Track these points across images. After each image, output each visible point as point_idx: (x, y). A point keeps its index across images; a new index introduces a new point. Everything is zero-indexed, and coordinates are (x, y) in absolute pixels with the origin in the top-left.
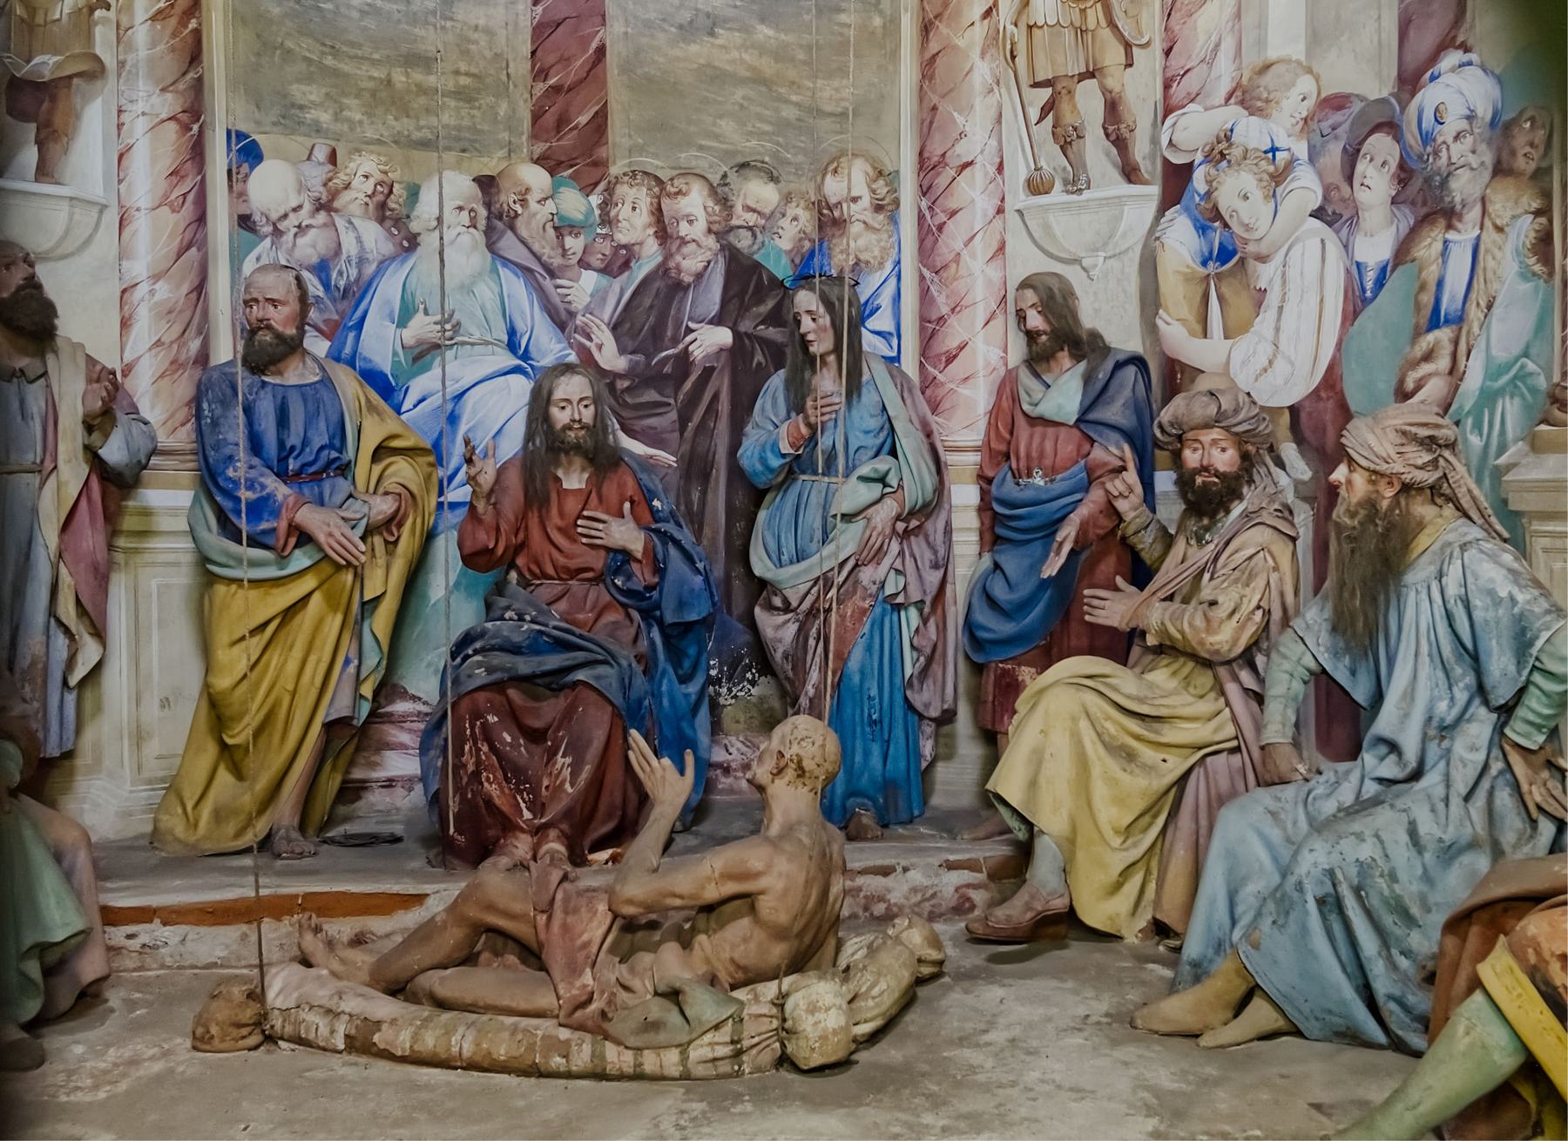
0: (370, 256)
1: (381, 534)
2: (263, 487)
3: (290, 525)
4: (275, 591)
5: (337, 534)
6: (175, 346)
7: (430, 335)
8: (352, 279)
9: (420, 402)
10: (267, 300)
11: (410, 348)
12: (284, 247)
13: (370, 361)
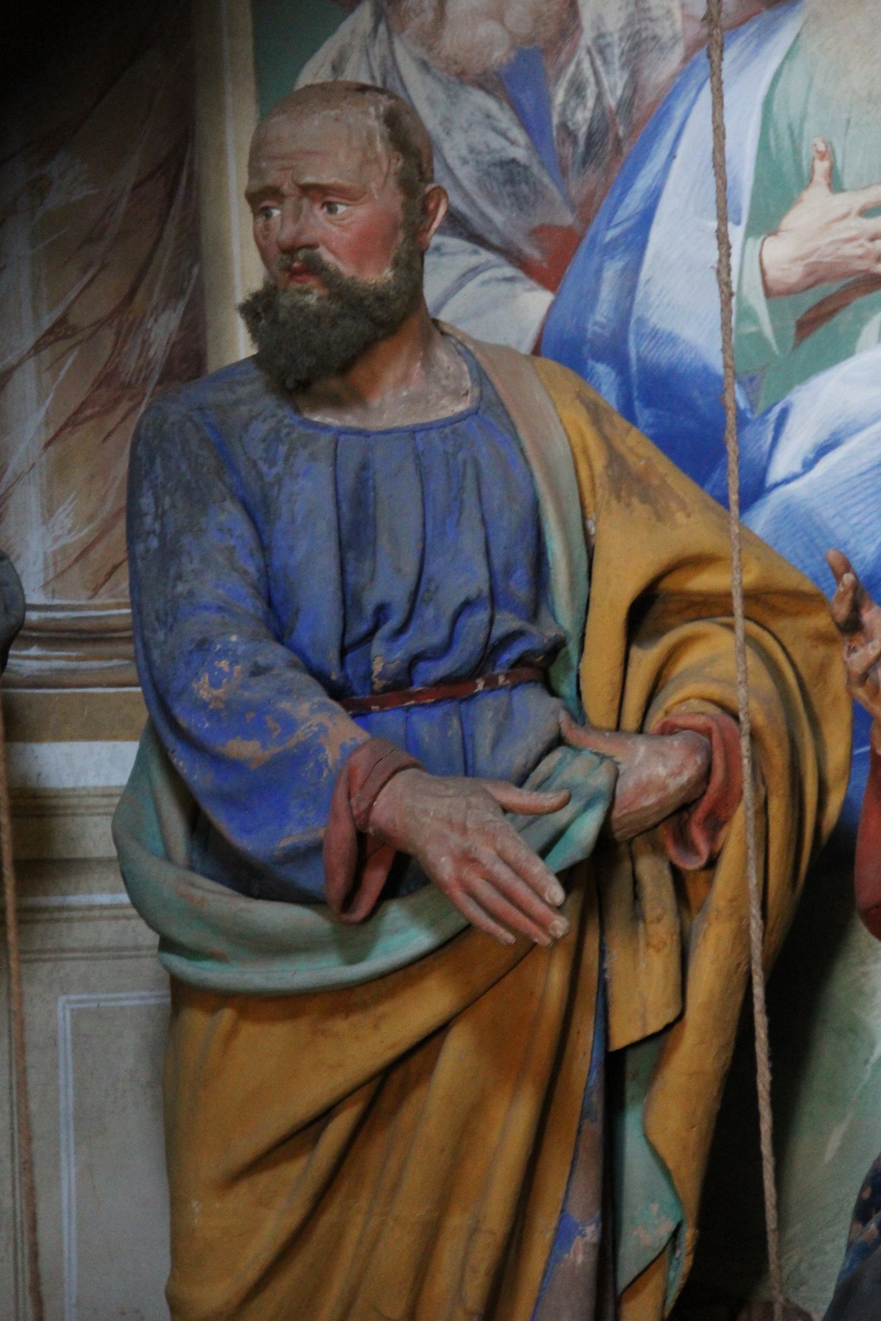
0: (665, 31)
1: (657, 849)
2: (289, 724)
3: (361, 837)
4: (341, 1025)
5: (486, 854)
6: (108, 337)
7: (850, 250)
8: (611, 102)
9: (823, 450)
10: (307, 190)
11: (790, 291)
12: (414, 24)
13: (672, 339)
